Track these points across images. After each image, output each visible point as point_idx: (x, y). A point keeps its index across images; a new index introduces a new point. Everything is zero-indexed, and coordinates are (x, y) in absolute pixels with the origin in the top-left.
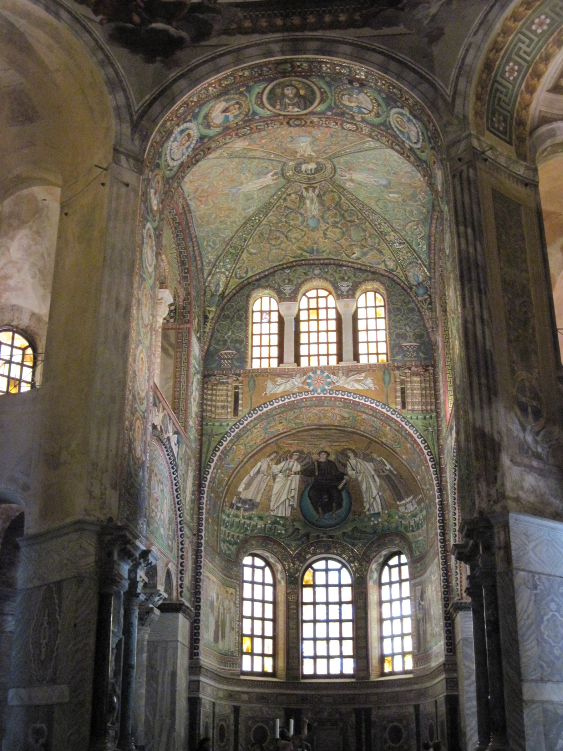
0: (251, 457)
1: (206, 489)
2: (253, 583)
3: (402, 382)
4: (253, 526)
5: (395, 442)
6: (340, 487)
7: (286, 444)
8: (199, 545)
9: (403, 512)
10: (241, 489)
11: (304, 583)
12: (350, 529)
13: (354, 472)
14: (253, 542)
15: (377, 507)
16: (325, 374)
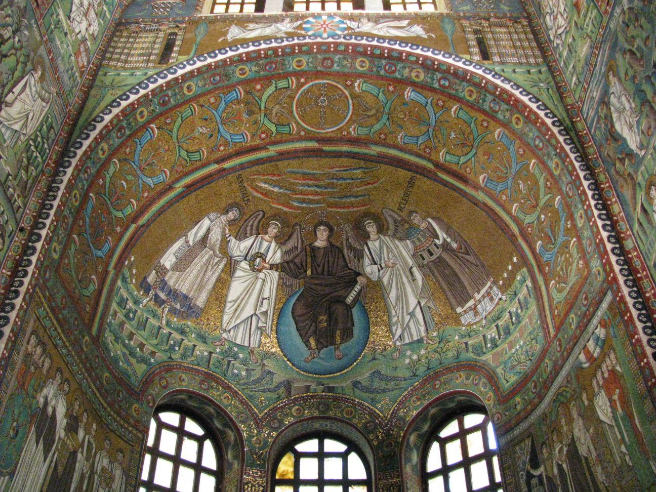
0: (190, 188)
1: (74, 162)
2: (177, 461)
3: (476, 32)
4: (186, 348)
5: (464, 145)
6: (349, 300)
7: (257, 189)
8: (27, 250)
9: (469, 325)
10: (168, 260)
11: (277, 477)
12: (368, 375)
13: (375, 267)
14: (184, 376)
15: (417, 330)
16: (337, 19)
